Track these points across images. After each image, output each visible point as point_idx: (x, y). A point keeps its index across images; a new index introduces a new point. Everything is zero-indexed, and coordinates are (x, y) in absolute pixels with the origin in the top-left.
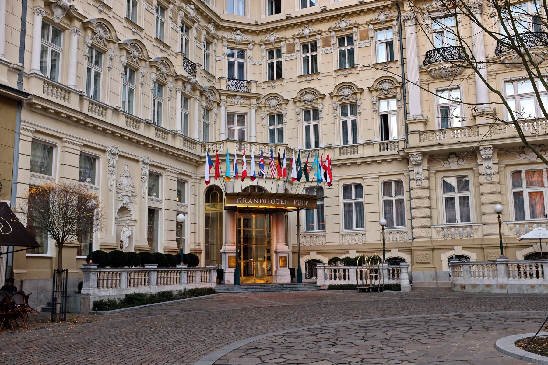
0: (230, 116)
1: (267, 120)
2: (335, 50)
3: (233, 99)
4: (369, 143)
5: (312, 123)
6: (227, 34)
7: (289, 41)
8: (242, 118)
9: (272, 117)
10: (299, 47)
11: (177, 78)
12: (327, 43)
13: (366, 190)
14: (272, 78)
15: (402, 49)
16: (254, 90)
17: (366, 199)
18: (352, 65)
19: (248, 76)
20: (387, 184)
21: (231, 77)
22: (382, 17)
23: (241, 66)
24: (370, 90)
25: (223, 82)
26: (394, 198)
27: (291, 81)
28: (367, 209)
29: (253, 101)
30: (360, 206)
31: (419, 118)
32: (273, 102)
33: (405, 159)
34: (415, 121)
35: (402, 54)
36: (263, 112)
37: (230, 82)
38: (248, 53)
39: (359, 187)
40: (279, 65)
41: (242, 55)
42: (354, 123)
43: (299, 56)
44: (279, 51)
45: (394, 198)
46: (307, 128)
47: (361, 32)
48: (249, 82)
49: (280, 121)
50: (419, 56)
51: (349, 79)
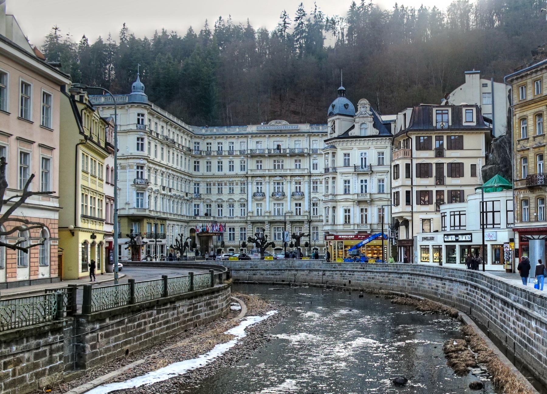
0: (195, 205)
1: (206, 206)
2: (228, 187)
3: (196, 200)
4: (237, 217)
5: (220, 209)
6: (194, 179)
7: (214, 182)
8: (198, 205)
9: (207, 205)
10: (217, 184)
11: (185, 200)
12: (226, 184)
13: (235, 230)
14: (207, 192)
15: (247, 190)
16: (202, 197)
17: (236, 232)
18: (233, 193)
19: (201, 192)
20: (241, 229)
21: (195, 193)
22: (242, 180)
23: (198, 188)
24: (238, 201)
25: (193, 195)
26: (243, 232)
27: (214, 195)
28: (235, 235)
29: (202, 200)
30: (234, 234)
31: (251, 211)
32: (208, 201)
33: (246, 222)
34: (250, 212)
35: (247, 191)
36: (205, 204)
37: (195, 195)
38: (201, 184)
39: (234, 229)
40: (210, 189)
41: (198, 185)
42: (233, 210)
43: (217, 187)
44: (210, 184)
45: (243, 232)
46: (219, 210)
47: (236, 183)
48: (201, 194)
49: (210, 207)
50: (252, 192)
51: (232, 197)
